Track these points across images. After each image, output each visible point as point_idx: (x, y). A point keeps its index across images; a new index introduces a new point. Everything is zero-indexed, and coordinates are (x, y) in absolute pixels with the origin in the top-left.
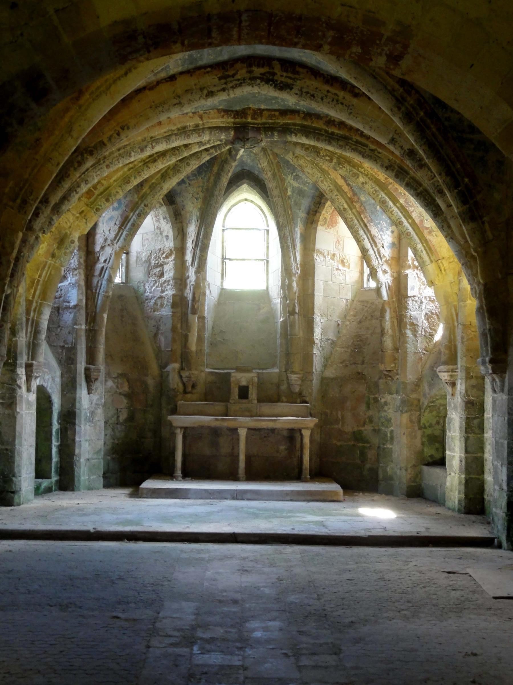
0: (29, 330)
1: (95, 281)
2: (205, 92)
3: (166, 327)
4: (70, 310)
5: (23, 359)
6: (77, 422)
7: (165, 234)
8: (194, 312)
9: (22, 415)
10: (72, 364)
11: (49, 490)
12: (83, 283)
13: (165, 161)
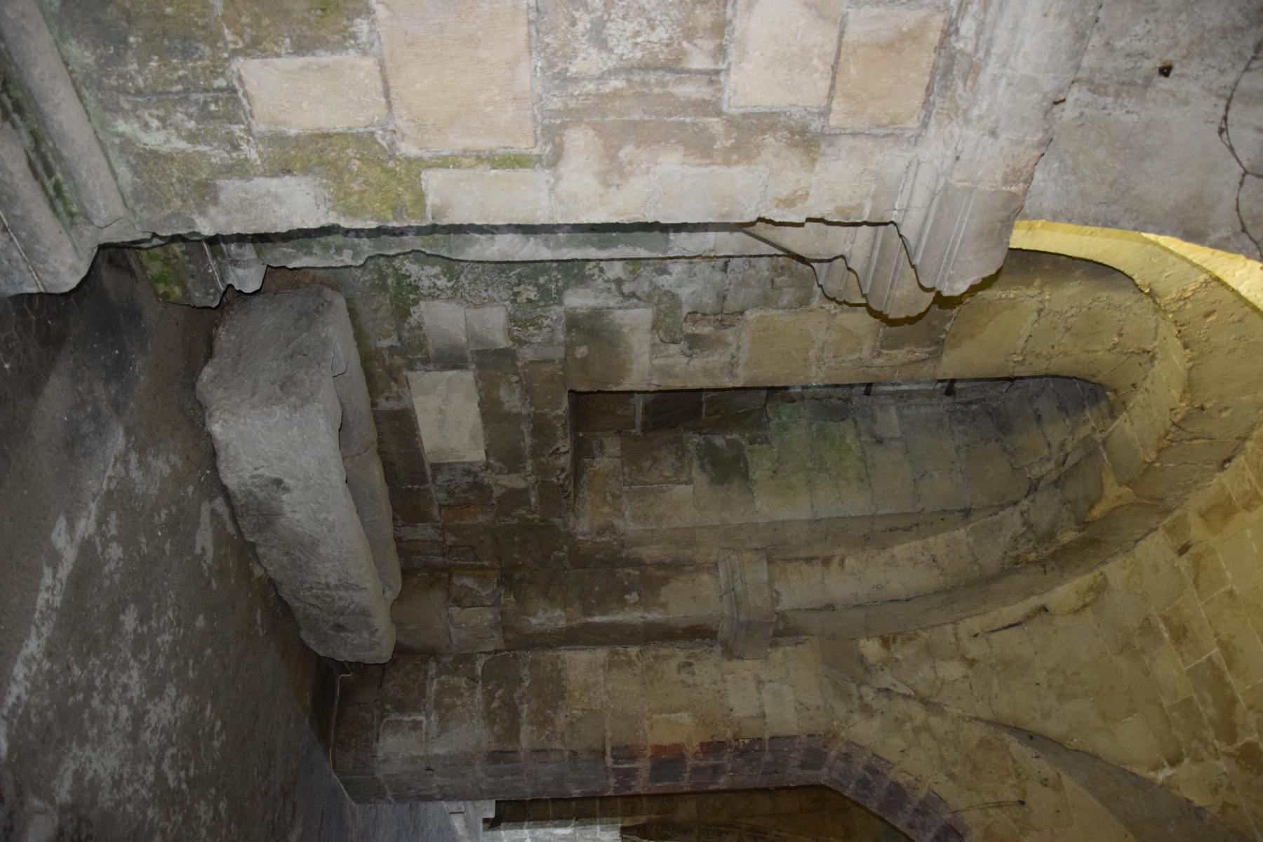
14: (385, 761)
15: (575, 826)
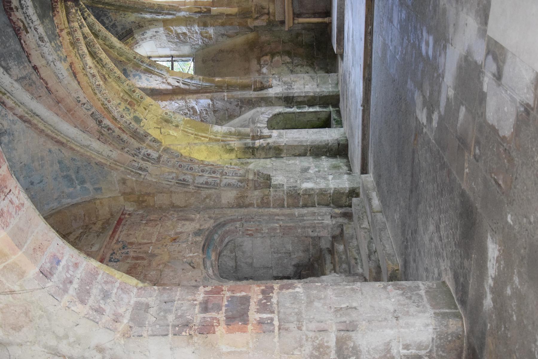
0: (229, 139)
1: (193, 88)
2: (40, 43)
3: (222, 30)
4: (215, 103)
5: (249, 141)
6: (292, 95)
7: (155, 34)
8: (209, 11)
9: (287, 141)
10: (252, 100)
11: (339, 112)
12: (195, 96)
13: (100, 52)
14: (428, 325)
15: (300, 189)
